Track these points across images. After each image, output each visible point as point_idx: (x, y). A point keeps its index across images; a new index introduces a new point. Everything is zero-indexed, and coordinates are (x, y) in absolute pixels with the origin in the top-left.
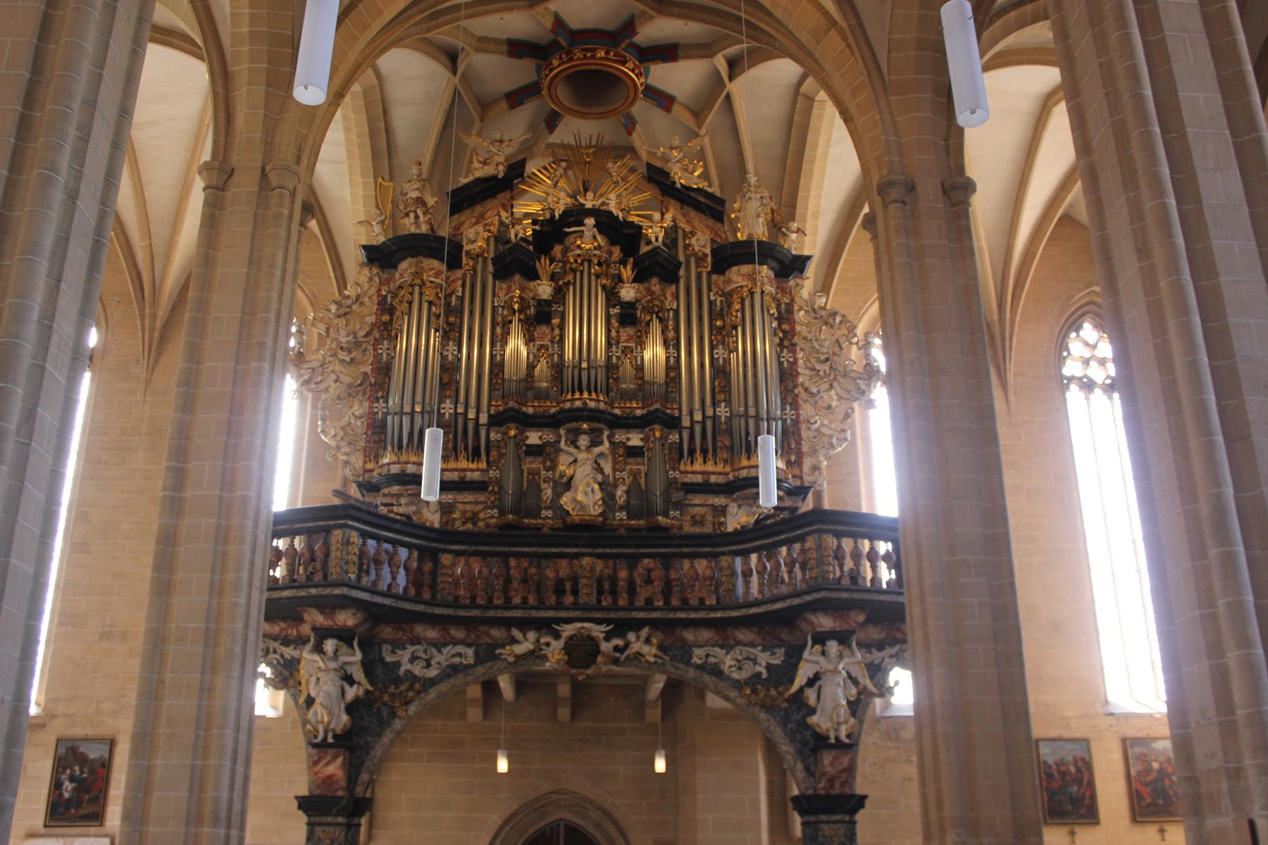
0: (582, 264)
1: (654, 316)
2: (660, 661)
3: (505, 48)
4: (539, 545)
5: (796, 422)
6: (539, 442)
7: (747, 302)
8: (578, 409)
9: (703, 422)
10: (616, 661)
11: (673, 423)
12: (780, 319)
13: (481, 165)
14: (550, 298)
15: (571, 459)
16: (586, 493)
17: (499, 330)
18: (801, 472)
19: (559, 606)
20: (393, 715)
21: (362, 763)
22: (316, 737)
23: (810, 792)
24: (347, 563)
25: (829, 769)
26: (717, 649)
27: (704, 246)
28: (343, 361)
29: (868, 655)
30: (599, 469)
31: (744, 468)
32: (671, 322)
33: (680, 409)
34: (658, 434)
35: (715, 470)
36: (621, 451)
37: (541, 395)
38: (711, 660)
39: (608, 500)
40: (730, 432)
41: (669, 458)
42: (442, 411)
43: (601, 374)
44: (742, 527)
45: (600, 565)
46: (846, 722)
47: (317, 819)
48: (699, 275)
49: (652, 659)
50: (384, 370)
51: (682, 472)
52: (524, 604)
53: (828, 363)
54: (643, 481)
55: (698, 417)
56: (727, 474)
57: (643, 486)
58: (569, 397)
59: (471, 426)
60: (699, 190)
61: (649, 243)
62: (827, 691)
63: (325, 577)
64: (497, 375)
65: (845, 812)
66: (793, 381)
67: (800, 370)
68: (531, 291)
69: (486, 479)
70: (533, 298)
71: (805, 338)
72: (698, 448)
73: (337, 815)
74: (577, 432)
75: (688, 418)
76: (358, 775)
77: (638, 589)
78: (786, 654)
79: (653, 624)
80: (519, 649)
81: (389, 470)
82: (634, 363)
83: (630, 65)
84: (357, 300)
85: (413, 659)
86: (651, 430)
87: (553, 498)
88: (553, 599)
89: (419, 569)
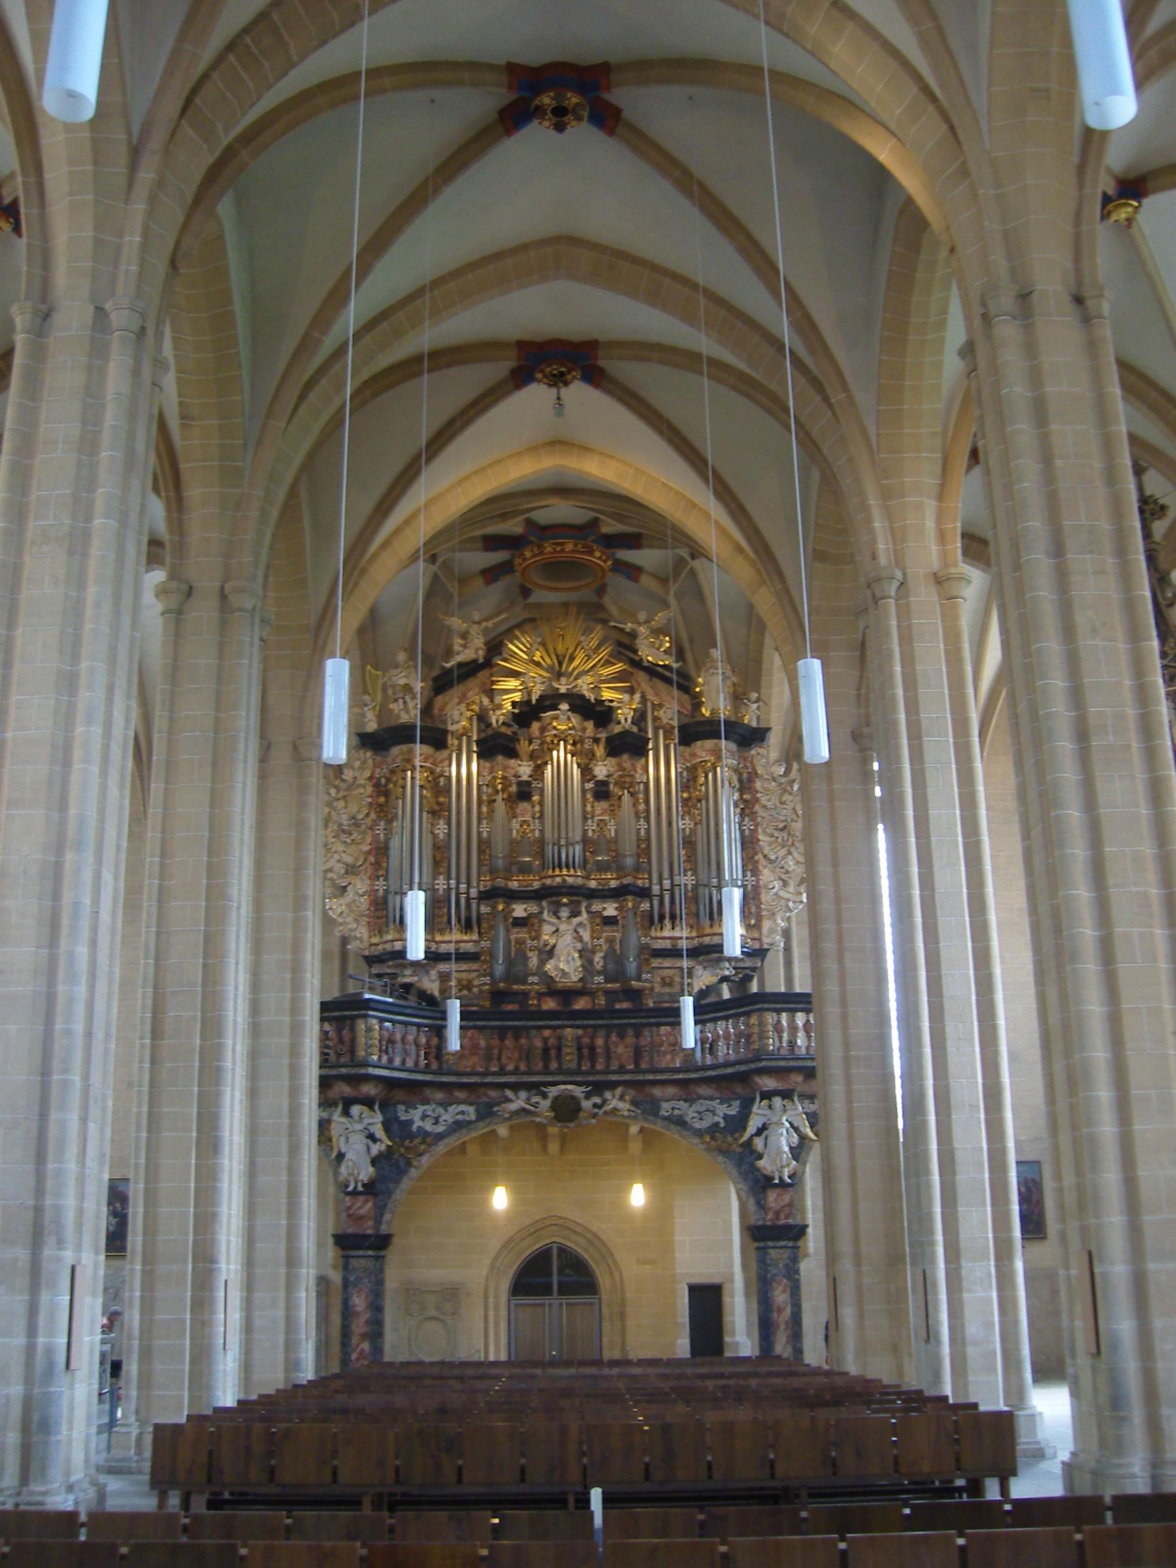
0: (558, 744)
1: (626, 791)
2: (633, 1114)
3: (480, 545)
4: (527, 1020)
5: (756, 888)
6: (524, 915)
7: (710, 776)
8: (559, 887)
9: (672, 891)
10: (595, 1116)
11: (645, 893)
12: (742, 791)
13: (461, 649)
14: (530, 779)
15: (554, 929)
16: (568, 962)
17: (484, 809)
18: (761, 934)
19: (546, 1071)
20: (409, 1164)
21: (385, 1206)
22: (347, 1186)
23: (760, 1223)
24: (371, 1046)
25: (773, 1205)
26: (681, 1102)
27: (672, 719)
28: (345, 842)
29: (811, 1105)
30: (580, 939)
31: (709, 935)
32: (641, 796)
33: (650, 879)
34: (630, 905)
35: (682, 935)
36: (598, 920)
37: (525, 869)
38: (676, 1112)
39: (588, 965)
40: (695, 899)
41: (642, 926)
42: (437, 887)
43: (578, 848)
44: (707, 987)
45: (580, 1032)
46: (788, 1165)
47: (353, 1253)
48: (667, 747)
49: (626, 1113)
50: (381, 850)
51: (653, 938)
52: (516, 1071)
53: (786, 831)
54: (617, 947)
55: (667, 883)
56: (692, 938)
57: (618, 952)
58: (550, 872)
59: (463, 901)
60: (665, 666)
61: (619, 723)
62: (771, 1140)
63: (352, 1059)
64: (484, 852)
65: (789, 1239)
66: (754, 849)
67: (760, 837)
68: (513, 768)
69: (477, 949)
70: (515, 776)
71: (764, 807)
72: (667, 915)
73: (369, 1248)
74: (559, 905)
75: (658, 887)
76: (382, 1215)
77: (613, 1055)
78: (741, 1104)
79: (626, 1084)
80: (513, 1107)
81: (393, 947)
82: (608, 836)
83: (598, 554)
84: (354, 783)
85: (424, 1117)
86: (625, 900)
87: (538, 966)
88: (540, 1066)
89: (428, 1042)
